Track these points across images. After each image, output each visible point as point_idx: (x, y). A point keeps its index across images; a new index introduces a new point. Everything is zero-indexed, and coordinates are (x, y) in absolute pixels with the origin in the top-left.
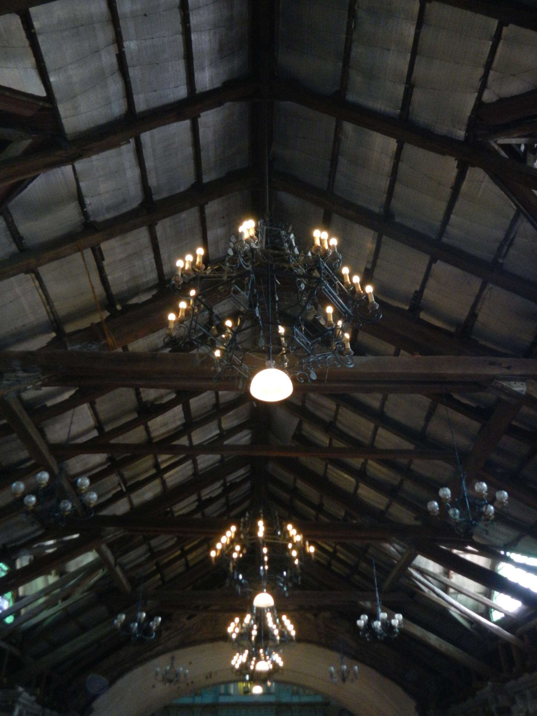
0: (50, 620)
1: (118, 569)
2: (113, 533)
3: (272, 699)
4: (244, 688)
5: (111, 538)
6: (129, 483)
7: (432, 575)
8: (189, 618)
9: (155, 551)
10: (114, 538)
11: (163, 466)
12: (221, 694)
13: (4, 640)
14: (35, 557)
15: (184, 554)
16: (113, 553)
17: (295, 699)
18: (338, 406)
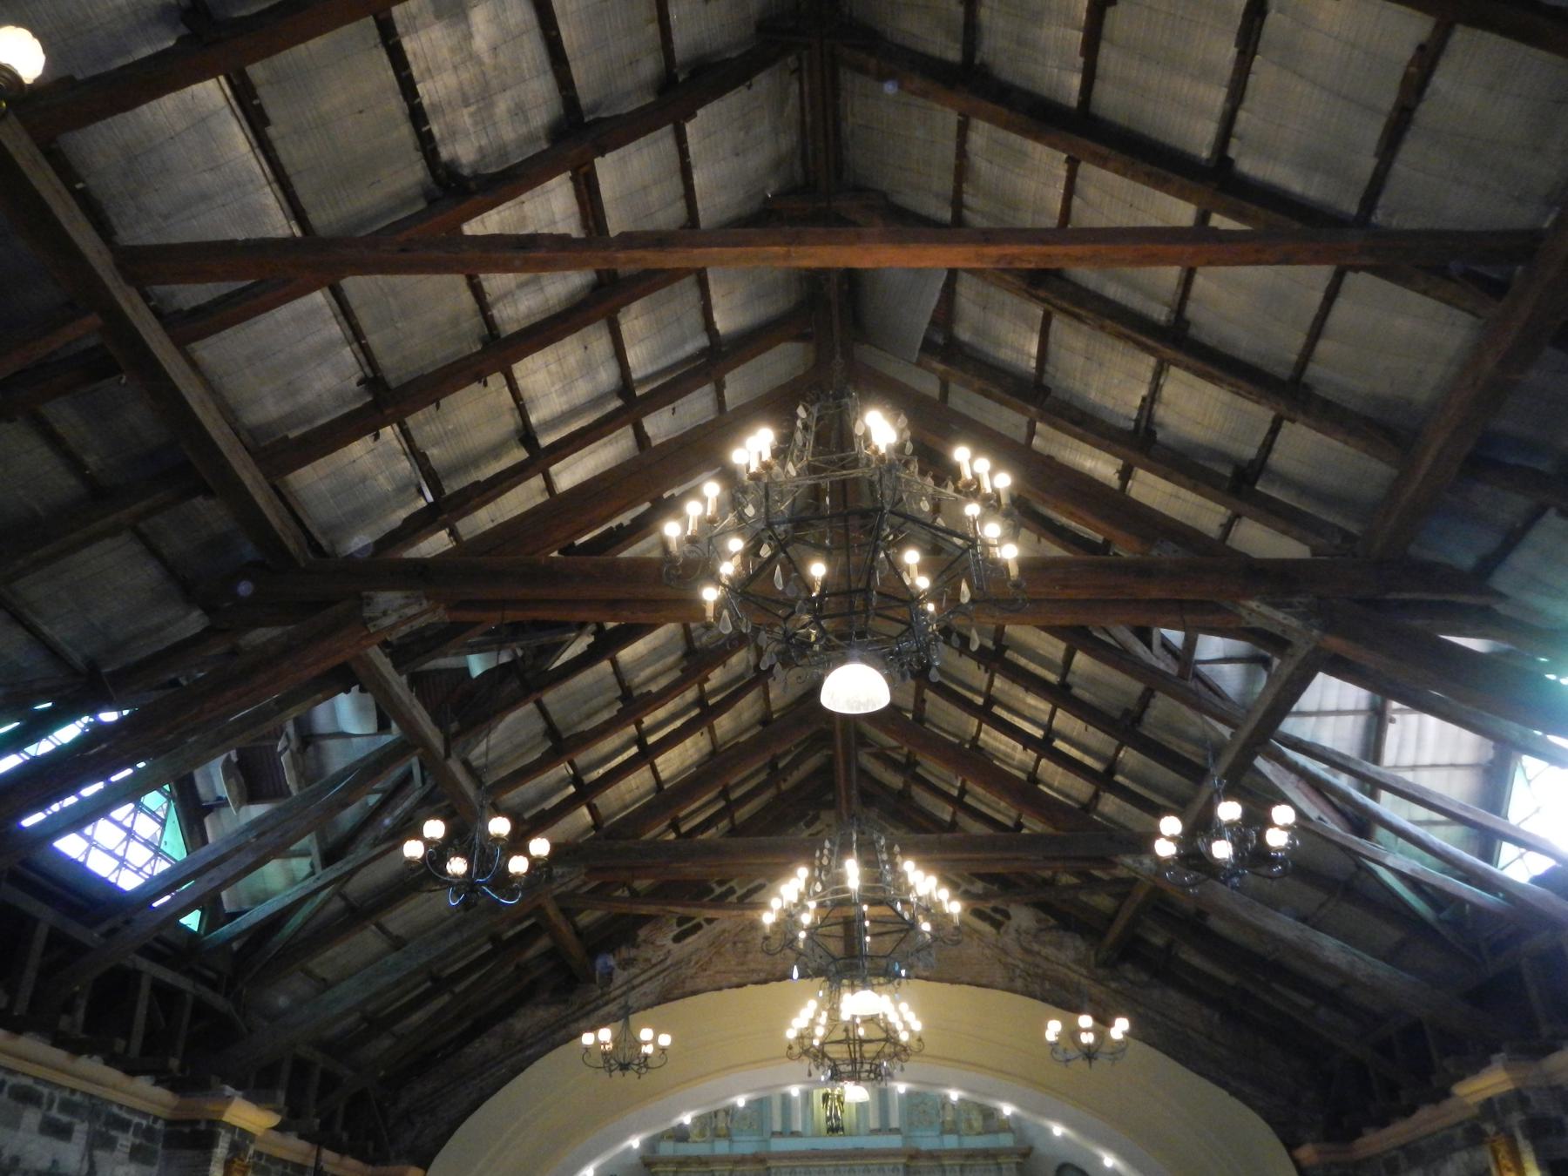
0: (297, 919)
1: (455, 766)
2: (393, 609)
3: (895, 1142)
4: (829, 1119)
5: (393, 627)
6: (452, 486)
7: (1338, 760)
8: (677, 939)
9: (565, 736)
10: (405, 629)
11: (545, 441)
12: (774, 1134)
13: (147, 951)
14: (240, 752)
15: (647, 754)
16: (438, 721)
17: (951, 1142)
18: (1073, 164)
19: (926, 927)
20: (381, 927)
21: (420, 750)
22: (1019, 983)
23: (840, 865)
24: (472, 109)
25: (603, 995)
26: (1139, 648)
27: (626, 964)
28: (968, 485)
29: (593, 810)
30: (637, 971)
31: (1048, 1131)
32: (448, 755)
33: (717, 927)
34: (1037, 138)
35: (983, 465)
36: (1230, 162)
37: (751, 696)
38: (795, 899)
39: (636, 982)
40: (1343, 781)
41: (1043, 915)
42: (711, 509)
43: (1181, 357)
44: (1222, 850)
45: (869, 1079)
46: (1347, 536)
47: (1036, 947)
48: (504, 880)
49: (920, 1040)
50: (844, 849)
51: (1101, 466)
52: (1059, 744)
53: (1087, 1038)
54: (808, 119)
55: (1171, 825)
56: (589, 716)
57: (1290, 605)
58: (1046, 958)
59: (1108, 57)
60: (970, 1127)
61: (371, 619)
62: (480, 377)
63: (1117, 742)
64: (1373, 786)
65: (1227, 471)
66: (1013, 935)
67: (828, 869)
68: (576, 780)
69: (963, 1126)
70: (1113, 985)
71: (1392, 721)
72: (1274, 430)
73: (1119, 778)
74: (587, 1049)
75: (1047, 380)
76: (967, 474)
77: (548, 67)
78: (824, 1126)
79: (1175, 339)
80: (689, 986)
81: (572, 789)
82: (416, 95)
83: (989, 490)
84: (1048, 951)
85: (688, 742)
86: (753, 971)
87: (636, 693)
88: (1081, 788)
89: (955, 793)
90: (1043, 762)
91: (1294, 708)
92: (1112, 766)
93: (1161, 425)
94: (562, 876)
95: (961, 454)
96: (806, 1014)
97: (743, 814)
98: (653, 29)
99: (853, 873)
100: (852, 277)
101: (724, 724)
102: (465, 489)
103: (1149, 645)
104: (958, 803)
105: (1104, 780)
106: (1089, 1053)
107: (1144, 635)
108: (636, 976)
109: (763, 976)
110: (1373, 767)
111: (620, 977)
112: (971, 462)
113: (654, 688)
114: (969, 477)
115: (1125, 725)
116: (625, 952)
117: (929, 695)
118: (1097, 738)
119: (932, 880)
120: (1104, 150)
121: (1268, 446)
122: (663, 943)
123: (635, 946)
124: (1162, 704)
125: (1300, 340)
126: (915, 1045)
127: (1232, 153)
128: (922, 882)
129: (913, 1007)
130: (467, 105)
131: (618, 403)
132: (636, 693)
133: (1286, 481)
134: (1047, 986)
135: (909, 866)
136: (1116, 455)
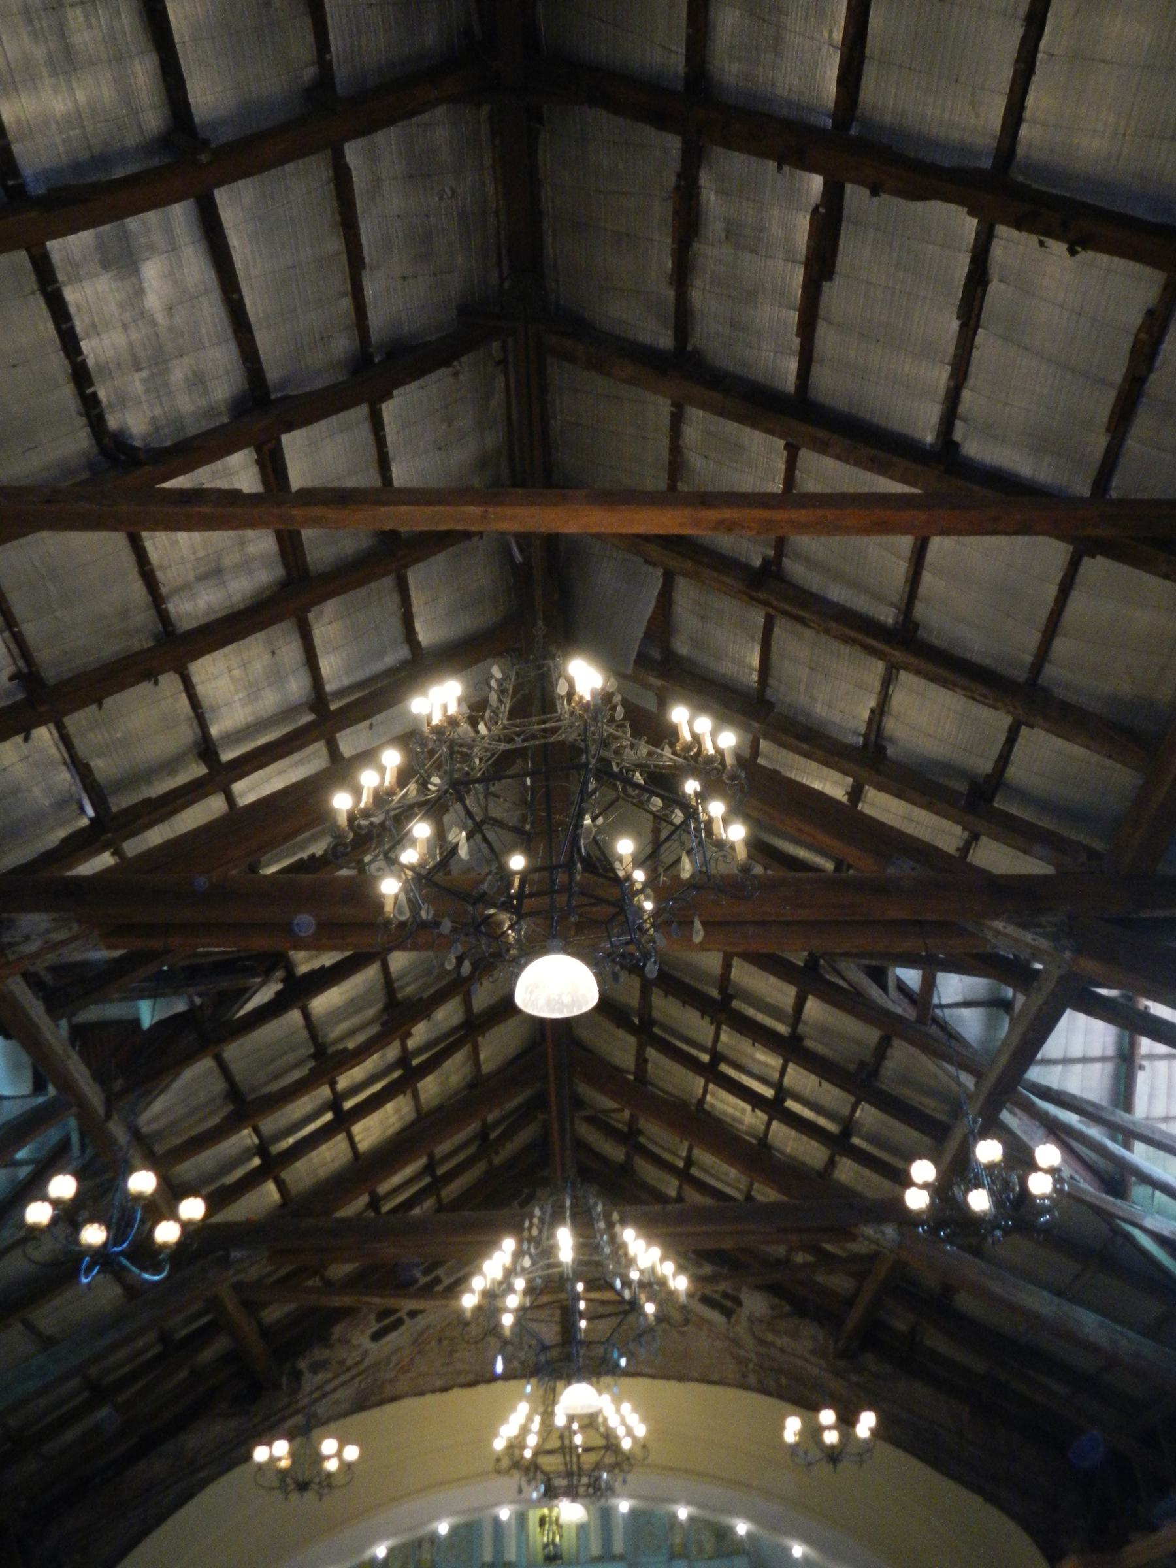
4: (546, 1546)
5: (37, 955)
6: (119, 803)
7: (1090, 1109)
8: (376, 1337)
11: (227, 756)
15: (343, 1121)
16: (101, 1077)
19: (650, 1308)
20: (30, 1326)
21: (74, 1110)
22: (752, 1379)
23: (552, 1236)
24: (144, 374)
25: (289, 1405)
26: (874, 992)
27: (316, 1368)
28: (688, 748)
29: (281, 1185)
30: (330, 1375)
31: (787, 1551)
32: (108, 1116)
33: (421, 1321)
34: (754, 425)
35: (704, 724)
36: (957, 445)
37: (460, 1057)
38: (499, 1275)
39: (328, 1387)
40: (1095, 1132)
41: (777, 1301)
42: (389, 779)
43: (913, 660)
44: (979, 1201)
45: (587, 1496)
46: (1092, 853)
47: (770, 1337)
48: (146, 1252)
49: (644, 1447)
50: (556, 1218)
51: (832, 785)
52: (790, 1104)
53: (831, 1437)
54: (515, 417)
55: (923, 1170)
56: (277, 1077)
57: (1040, 926)
58: (782, 1350)
59: (826, 338)
60: (701, 1550)
61: (10, 945)
62: (152, 675)
63: (852, 1099)
64: (1128, 1135)
65: (962, 787)
66: (745, 1324)
67: (537, 1241)
68: (262, 1150)
69: (694, 1550)
70: (854, 1378)
71: (1142, 1068)
72: (1011, 741)
73: (856, 1141)
74: (260, 1467)
75: (770, 694)
76: (685, 735)
77: (229, 333)
78: (540, 1557)
79: (902, 641)
80: (389, 1391)
81: (256, 1161)
82: (79, 351)
83: (711, 751)
84: (783, 1341)
85: (390, 1107)
86: (459, 1373)
87: (330, 1050)
88: (813, 1153)
89: (681, 1164)
90: (775, 1124)
91: (1039, 1056)
92: (848, 1126)
93: (891, 740)
94: (241, 1260)
95: (679, 714)
96: (517, 1423)
97: (451, 1190)
98: (346, 303)
99: (565, 1243)
100: (552, 541)
101: (430, 1087)
102: (135, 806)
103: (884, 987)
104: (684, 1175)
105: (839, 1143)
106: (833, 1455)
107: (879, 976)
108: (329, 1381)
109: (470, 1378)
110: (1127, 1116)
111: (310, 1381)
112: (690, 724)
113: (351, 1045)
114: (689, 738)
115: (860, 1078)
116: (320, 1354)
117: (651, 1053)
118: (832, 1095)
119: (656, 1252)
120: (822, 434)
121: (1004, 759)
122: (360, 1343)
123: (329, 1346)
124: (901, 1054)
125: (1033, 639)
126: (639, 1453)
127: (958, 436)
128: (644, 1254)
129: (636, 1409)
130: (138, 369)
131: (309, 717)
132: (330, 1050)
133: (1022, 795)
134: (783, 1381)
135: (629, 1236)
136: (845, 772)
